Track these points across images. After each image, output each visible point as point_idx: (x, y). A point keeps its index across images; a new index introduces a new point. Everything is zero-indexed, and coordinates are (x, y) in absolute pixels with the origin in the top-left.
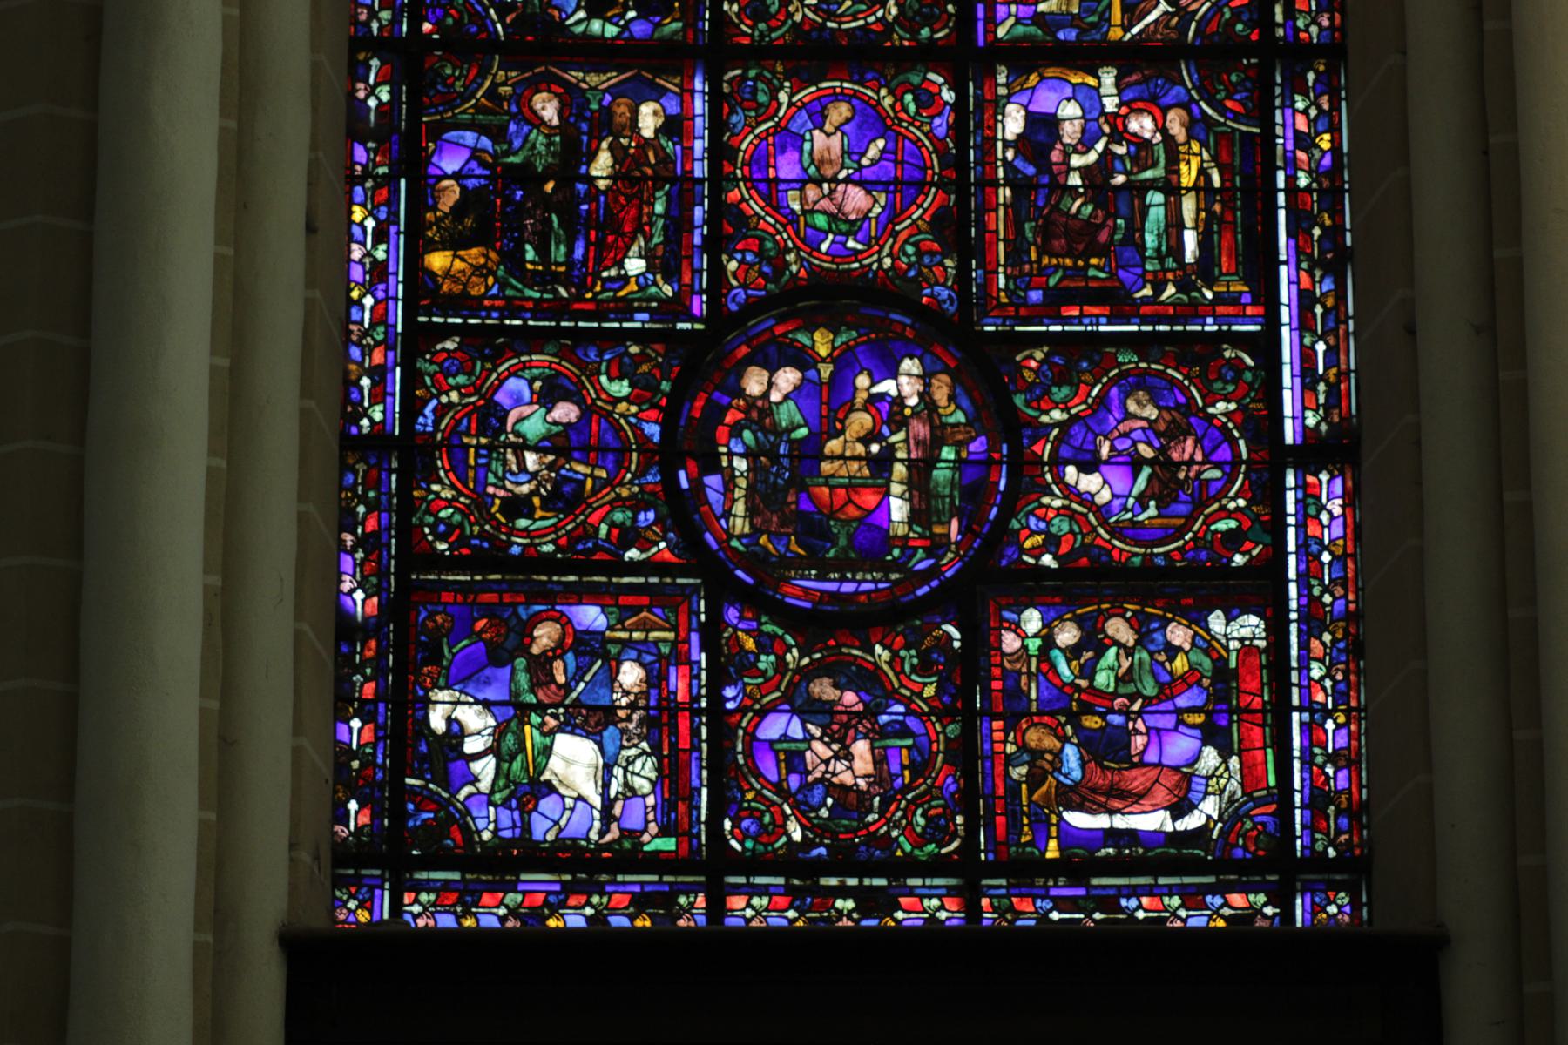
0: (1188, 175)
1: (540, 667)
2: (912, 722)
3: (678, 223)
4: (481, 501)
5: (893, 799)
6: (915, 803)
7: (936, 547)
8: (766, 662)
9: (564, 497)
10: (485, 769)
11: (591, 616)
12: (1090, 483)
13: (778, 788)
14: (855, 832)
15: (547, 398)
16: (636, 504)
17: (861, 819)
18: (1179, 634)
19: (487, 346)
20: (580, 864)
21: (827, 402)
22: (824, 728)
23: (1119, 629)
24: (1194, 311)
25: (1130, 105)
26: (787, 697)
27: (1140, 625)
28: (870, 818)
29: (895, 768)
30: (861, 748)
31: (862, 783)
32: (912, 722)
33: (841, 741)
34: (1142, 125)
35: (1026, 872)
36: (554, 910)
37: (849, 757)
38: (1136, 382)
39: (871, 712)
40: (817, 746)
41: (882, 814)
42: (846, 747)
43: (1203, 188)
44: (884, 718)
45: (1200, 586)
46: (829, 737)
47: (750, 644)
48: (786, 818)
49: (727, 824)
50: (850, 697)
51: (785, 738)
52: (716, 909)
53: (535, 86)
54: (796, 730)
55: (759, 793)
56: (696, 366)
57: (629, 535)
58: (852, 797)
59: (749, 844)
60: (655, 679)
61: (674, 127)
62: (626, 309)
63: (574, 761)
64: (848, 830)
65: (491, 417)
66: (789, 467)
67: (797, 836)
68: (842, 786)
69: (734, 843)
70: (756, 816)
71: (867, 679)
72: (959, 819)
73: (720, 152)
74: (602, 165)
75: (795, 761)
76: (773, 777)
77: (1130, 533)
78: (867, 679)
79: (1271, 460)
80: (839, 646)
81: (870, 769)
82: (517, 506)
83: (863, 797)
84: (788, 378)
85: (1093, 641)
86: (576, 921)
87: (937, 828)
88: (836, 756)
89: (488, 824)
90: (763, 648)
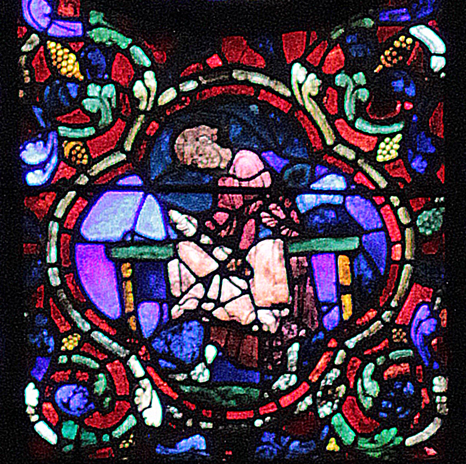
2: (356, 207)
5: (322, 347)
6: (361, 354)
8: (98, 98)
13: (120, 328)
14: (255, 406)
17: (266, 385)
22: (202, 217)
26: (137, 163)
28: (281, 383)
29: (326, 292)
30: (267, 255)
31: (268, 319)
32: (356, 207)
33: (232, 242)
37: (245, 271)
39: (284, 189)
40: (188, 250)
41: (303, 372)
42: (240, 254)
44: (308, 200)
46: (212, 235)
47: (70, 65)
48: (134, 382)
49: (31, 395)
50: (247, 162)
51: (132, 238)
54: (152, 224)
55: (86, 338)
58: (251, 346)
59: (70, 430)
64: (243, 404)
67: (154, 417)
68: (233, 325)
69: (44, 430)
70: (82, 378)
71: (277, 130)
72: (439, 384)
75: (148, 277)
76: (112, 310)
78: (277, 130)
80: (228, 68)
81: (282, 292)
83: (271, 344)
87: (400, 399)
88: (223, 271)
90: (92, 73)
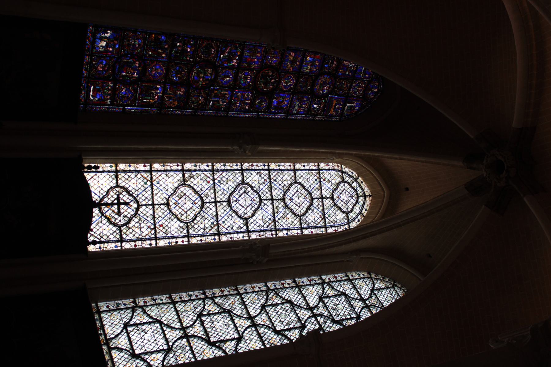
0: (151, 101)
1: (113, 41)
3: (154, 57)
4: (129, 37)
7: (120, 77)
9: (129, 45)
10: (103, 36)
11: (117, 46)
12: (124, 91)
15: (139, 44)
16: (127, 51)
18: (108, 97)
19: (144, 39)
20: (93, 43)
21: (135, 69)
23: (110, 92)
24: (139, 100)
25: (158, 97)
27: (110, 94)
34: (156, 97)
35: (88, 83)
36: (89, 40)
38: (133, 95)
39: (105, 70)
43: (150, 102)
45: (113, 100)
52: (87, 55)
53: (169, 46)
56: (140, 57)
57: (124, 51)
60: (110, 51)
61: (163, 57)
62: (146, 52)
63: (104, 44)
65: (138, 39)
66: (129, 65)
73: (160, 61)
74: (160, 51)
77: (119, 93)
79: (124, 106)
82: (129, 41)
84: (137, 65)
85: (108, 90)
86: (87, 42)
89: (98, 35)
